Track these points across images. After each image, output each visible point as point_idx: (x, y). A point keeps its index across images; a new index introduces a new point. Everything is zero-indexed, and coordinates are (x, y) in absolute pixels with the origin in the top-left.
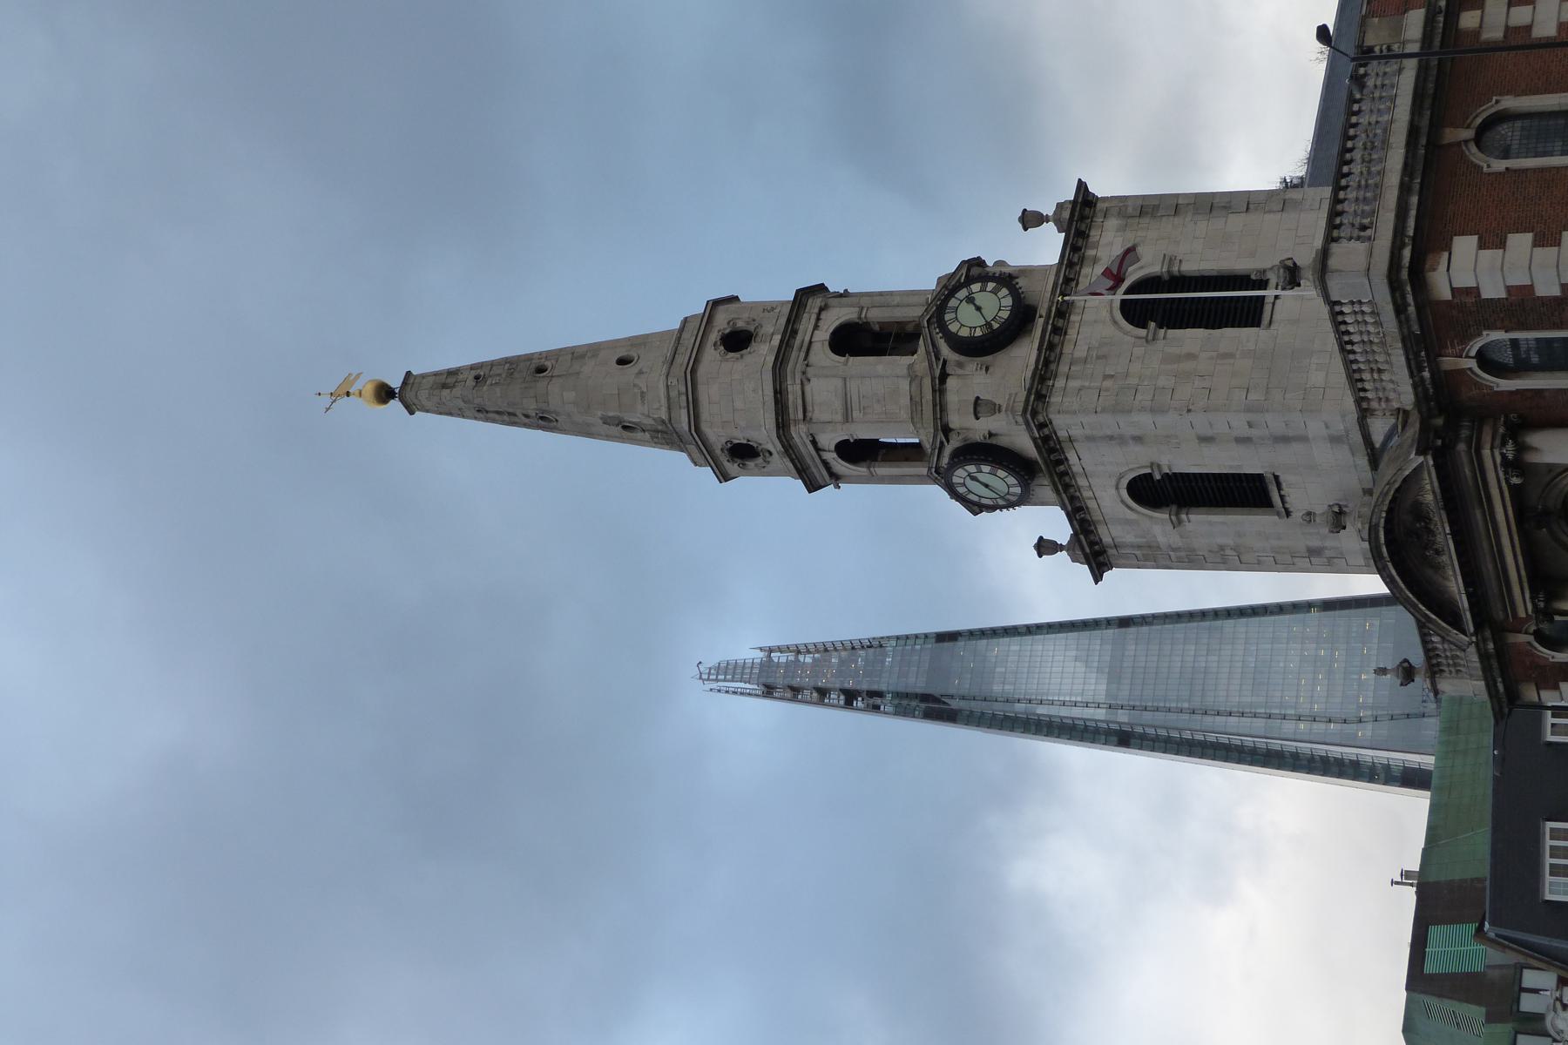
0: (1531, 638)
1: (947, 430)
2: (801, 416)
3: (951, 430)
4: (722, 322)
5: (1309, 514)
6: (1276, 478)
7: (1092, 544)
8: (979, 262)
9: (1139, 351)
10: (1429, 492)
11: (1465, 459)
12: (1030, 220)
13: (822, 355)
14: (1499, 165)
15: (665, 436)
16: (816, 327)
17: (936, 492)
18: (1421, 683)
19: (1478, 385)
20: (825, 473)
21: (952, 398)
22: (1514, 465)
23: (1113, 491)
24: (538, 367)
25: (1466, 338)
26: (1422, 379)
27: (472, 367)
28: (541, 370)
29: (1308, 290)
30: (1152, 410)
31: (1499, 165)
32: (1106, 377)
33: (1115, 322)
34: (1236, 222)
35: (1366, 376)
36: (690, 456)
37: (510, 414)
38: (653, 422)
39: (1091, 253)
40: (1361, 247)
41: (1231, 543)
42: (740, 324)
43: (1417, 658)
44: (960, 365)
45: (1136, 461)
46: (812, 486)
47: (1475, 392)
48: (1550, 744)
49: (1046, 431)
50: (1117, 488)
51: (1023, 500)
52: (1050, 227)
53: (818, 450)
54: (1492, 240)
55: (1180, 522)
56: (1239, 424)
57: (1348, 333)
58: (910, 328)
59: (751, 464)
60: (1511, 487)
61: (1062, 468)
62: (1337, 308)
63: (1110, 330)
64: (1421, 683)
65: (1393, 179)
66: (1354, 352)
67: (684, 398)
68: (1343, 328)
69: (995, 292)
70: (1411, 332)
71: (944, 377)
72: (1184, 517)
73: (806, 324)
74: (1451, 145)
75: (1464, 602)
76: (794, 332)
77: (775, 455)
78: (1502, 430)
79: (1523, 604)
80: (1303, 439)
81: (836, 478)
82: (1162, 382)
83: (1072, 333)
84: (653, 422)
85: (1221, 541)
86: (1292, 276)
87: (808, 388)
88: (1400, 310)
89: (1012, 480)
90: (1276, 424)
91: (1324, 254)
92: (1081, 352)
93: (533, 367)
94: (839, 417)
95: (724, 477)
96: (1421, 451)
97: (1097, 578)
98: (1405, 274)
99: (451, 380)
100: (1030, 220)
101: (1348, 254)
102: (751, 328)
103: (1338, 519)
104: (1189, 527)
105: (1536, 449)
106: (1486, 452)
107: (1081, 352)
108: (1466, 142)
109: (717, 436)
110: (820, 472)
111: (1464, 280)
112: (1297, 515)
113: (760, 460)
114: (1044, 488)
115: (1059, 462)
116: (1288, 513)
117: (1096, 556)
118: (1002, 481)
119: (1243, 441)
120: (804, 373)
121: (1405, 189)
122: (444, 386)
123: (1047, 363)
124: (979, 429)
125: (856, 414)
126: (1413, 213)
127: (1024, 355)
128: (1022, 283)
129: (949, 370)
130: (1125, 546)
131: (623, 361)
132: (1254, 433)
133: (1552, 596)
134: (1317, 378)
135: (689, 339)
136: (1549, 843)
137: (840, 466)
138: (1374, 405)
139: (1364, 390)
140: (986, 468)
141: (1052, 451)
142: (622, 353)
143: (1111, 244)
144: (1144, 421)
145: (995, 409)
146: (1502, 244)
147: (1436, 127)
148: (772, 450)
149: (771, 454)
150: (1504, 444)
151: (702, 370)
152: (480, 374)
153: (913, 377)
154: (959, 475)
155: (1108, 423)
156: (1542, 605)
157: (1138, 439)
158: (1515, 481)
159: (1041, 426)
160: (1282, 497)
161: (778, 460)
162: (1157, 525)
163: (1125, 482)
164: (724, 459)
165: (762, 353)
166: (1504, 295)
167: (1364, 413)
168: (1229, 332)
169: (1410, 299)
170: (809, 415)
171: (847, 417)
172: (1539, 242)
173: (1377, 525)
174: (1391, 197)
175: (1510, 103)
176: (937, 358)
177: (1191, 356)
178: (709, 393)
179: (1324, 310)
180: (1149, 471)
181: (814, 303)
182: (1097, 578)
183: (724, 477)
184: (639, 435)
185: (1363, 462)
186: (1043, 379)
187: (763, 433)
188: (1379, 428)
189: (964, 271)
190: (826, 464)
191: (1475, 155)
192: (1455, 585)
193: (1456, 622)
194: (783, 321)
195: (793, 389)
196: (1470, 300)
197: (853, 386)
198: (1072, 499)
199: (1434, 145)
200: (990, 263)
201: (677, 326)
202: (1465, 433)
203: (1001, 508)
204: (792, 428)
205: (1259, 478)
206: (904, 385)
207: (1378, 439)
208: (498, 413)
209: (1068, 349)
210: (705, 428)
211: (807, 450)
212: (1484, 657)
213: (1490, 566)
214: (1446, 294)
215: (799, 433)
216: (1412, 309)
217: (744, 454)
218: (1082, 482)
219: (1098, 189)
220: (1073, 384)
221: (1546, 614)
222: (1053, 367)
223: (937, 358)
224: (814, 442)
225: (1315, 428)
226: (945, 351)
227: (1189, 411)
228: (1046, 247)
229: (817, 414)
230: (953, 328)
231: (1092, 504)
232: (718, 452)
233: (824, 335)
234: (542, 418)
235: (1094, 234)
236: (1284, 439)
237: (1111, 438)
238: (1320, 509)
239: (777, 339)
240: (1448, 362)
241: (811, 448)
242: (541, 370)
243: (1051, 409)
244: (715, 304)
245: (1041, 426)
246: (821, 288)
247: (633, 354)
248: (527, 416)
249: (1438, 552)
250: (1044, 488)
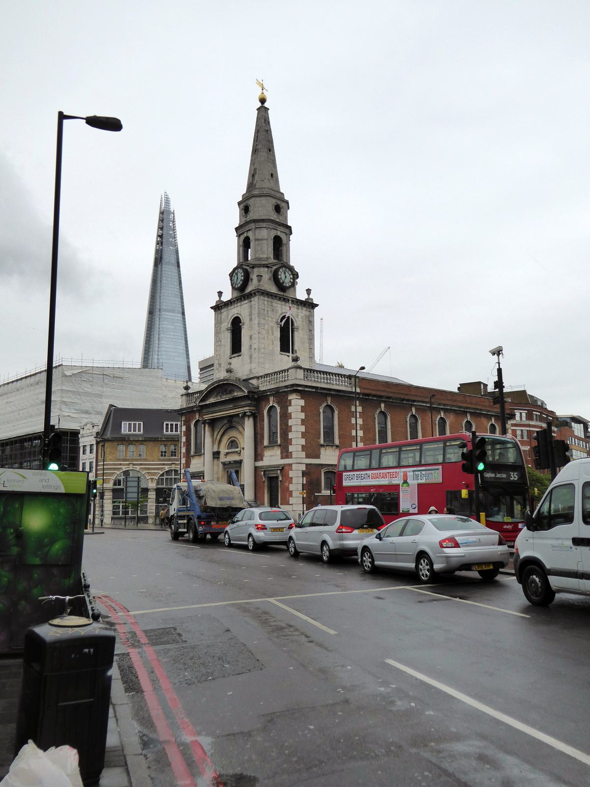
0: (197, 419)
1: (253, 268)
2: (257, 227)
4: (283, 205)
5: (231, 364)
6: (240, 355)
7: (221, 306)
8: (298, 277)
9: (274, 320)
10: (237, 394)
11: (246, 403)
12: (309, 291)
13: (273, 233)
14: (321, 411)
15: (251, 186)
16: (281, 232)
17: (235, 264)
18: (184, 392)
19: (266, 406)
20: (240, 233)
21: (262, 269)
22: (244, 414)
23: (236, 313)
24: (270, 149)
25: (278, 403)
26: (267, 392)
27: (270, 129)
28: (270, 150)
29: (291, 364)
30: (259, 323)
31: (321, 411)
32: (268, 311)
33: (282, 314)
34: (307, 345)
35: (268, 378)
36: (245, 194)
37: (257, 140)
38: (255, 183)
39: (300, 307)
40: (302, 377)
41: (222, 343)
42: (282, 210)
43: (190, 391)
44: (271, 272)
45: (245, 318)
46: (237, 229)
47: (263, 405)
48: (163, 423)
49: (253, 295)
50: (237, 314)
51: (233, 288)
52: (306, 297)
53: (247, 231)
54: (303, 409)
55: (228, 330)
56: (255, 346)
57: (280, 374)
58: (280, 258)
59: (243, 212)
60: (238, 414)
61: (243, 299)
62: (286, 371)
63: (280, 312)
64: (184, 392)
65: (318, 385)
66: (274, 375)
67: (262, 193)
68: (281, 373)
69: (290, 281)
70: (280, 389)
71: (268, 267)
72: (229, 331)
73: (282, 229)
74: (327, 398)
75: (207, 402)
76: (280, 225)
77: (245, 219)
78: (254, 412)
79: (207, 417)
80: (251, 362)
81: (239, 236)
82: (266, 326)
83: (279, 302)
84: (255, 183)
85: (222, 341)
86: (296, 360)
87: (263, 229)
88: (286, 387)
89: (239, 285)
90: (255, 355)
91: (300, 367)
92: (274, 305)
93: (270, 148)
94: (256, 237)
95: (239, 204)
96: (249, 392)
97: (212, 308)
98: (295, 388)
99: (267, 123)
100: (309, 291)
101: (300, 374)
102: (281, 213)
103: (229, 371)
104: (227, 333)
105: (249, 419)
106: (248, 408)
107: (274, 305)
108: (327, 403)
109: (251, 202)
110: (241, 232)
111: (293, 402)
112: (230, 361)
113: (244, 214)
114: (236, 294)
115: (244, 298)
116: (230, 358)
117: (218, 307)
118: (239, 283)
119: (251, 346)
120: (269, 228)
121: (316, 388)
122: (265, 120)
123: (272, 295)
124: (254, 277)
125: (257, 242)
126: (310, 390)
127: (273, 289)
128: (292, 289)
129: (270, 269)
130: (221, 315)
131: (272, 175)
132: (253, 350)
133: (208, 423)
134: (267, 366)
135: (278, 195)
136: (137, 423)
137: (242, 237)
138: (260, 380)
139: (264, 378)
140: (242, 278)
141: (248, 296)
142: (274, 175)
143: (302, 313)
144: (256, 321)
145: (259, 281)
146: (302, 411)
147: (331, 395)
148: (248, 218)
149: (246, 217)
150: (250, 412)
151: (269, 198)
152: (268, 131)
153: (268, 258)
154: (240, 270)
155: (255, 312)
156: (207, 421)
157: (251, 319)
158: (240, 415)
159: (255, 293)
160: (235, 357)
161: (244, 220)
162: (227, 324)
163: (239, 316)
164: (245, 204)
165: (274, 216)
166: (289, 412)
167: (258, 378)
168: (279, 343)
169: (289, 389)
170: (257, 229)
171: (256, 240)
172: (302, 420)
173: (228, 381)
174: (314, 385)
175: (336, 413)
176: (273, 265)
177: (273, 333)
178: (263, 200)
179: (286, 368)
180: (242, 322)
181: (287, 231)
182: (212, 308)
183: (239, 204)
184: (251, 179)
185: (245, 378)
186: (267, 294)
187: (252, 215)
188: (254, 382)
189: (296, 273)
190: (243, 233)
191: (324, 404)
192: (212, 400)
193: (202, 401)
194: (283, 222)
195: (264, 225)
196: (288, 404)
197: (265, 242)
198: (234, 301)
199: (326, 395)
200: (297, 280)
201: (282, 191)
202: (253, 403)
203: (231, 282)
204: (253, 224)
205: (240, 351)
206: (265, 256)
207: (251, 381)
208: (257, 136)
209: (275, 301)
210: (254, 198)
211: (247, 228)
212: (193, 407)
213: (217, 409)
214: (289, 398)
215: (252, 226)
216: (286, 390)
218: (239, 304)
219: (316, 309)
220: (266, 303)
221: (204, 422)
222: (271, 297)
223: (273, 265)
224: (249, 230)
225: (254, 365)
226: (274, 268)
227: (259, 333)
228: (301, 295)
229: (257, 231)
230: (281, 270)
231: (233, 307)
232: (247, 202)
233: (279, 234)
234: (256, 151)
235: (304, 309)
236: (251, 357)
237: (251, 312)
238: (232, 367)
239: (277, 220)
240: (271, 399)
241: (248, 229)
242: (270, 150)
243: (259, 297)
244: (287, 202)
245: (255, 293)
246: (291, 233)
247: (274, 178)
248: (256, 145)
249: (221, 396)
250: (236, 294)
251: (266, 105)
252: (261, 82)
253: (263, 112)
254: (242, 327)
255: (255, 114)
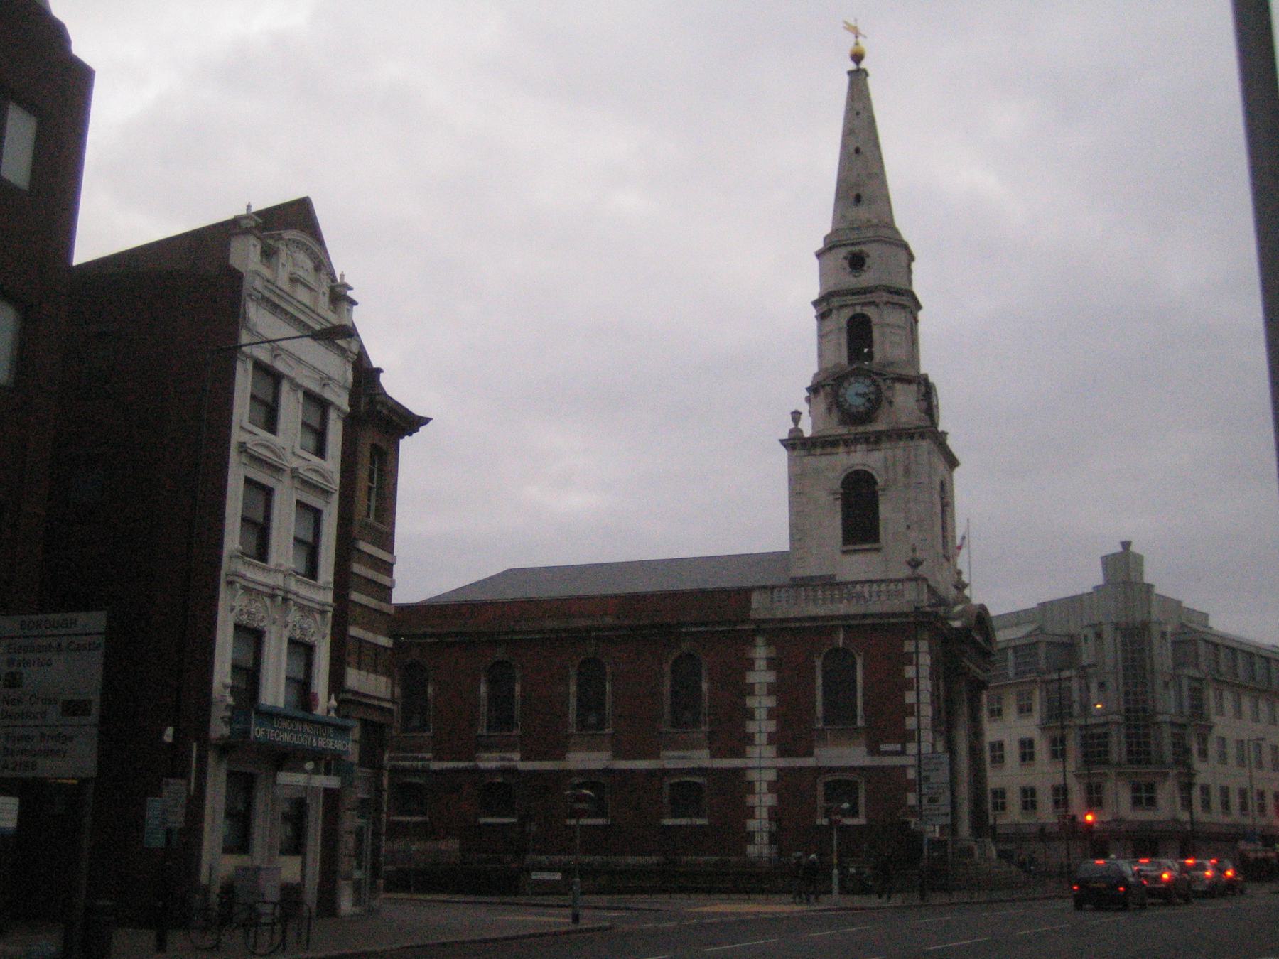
3: (894, 382)
97: (783, 442)
113: (849, 269)
137: (846, 314)
161: (850, 281)
164: (856, 249)
182: (783, 442)
190: (853, 305)
211: (869, 298)
217: (857, 262)
251: (863, 65)
252: (853, 24)
253: (858, 78)
254: (880, 493)
255: (846, 80)
